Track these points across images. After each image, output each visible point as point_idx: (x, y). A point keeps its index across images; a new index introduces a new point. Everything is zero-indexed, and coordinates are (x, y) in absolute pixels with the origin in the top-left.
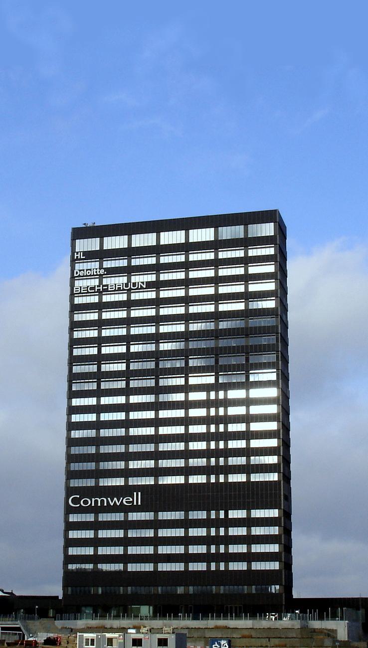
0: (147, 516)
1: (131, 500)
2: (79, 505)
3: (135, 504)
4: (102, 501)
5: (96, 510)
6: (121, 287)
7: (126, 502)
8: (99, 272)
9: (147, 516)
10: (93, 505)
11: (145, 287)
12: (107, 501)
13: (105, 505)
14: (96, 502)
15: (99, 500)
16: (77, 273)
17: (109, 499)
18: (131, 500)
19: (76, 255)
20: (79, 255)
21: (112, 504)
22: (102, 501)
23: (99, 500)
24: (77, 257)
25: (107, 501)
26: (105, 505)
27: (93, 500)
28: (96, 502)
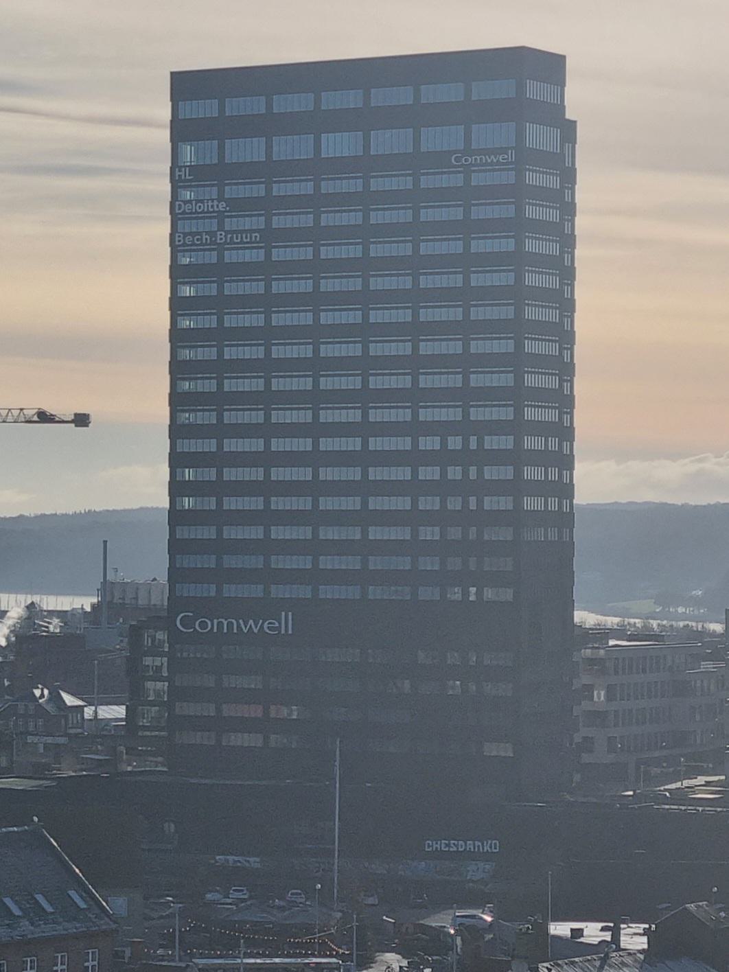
1: (277, 625)
2: (192, 630)
3: (283, 632)
4: (230, 625)
7: (268, 627)
8: (218, 206)
10: (215, 630)
12: (238, 622)
13: (235, 631)
14: (220, 624)
15: (225, 623)
17: (241, 621)
18: (277, 625)
20: (183, 173)
22: (230, 625)
23: (225, 623)
25: (238, 622)
27: (215, 621)
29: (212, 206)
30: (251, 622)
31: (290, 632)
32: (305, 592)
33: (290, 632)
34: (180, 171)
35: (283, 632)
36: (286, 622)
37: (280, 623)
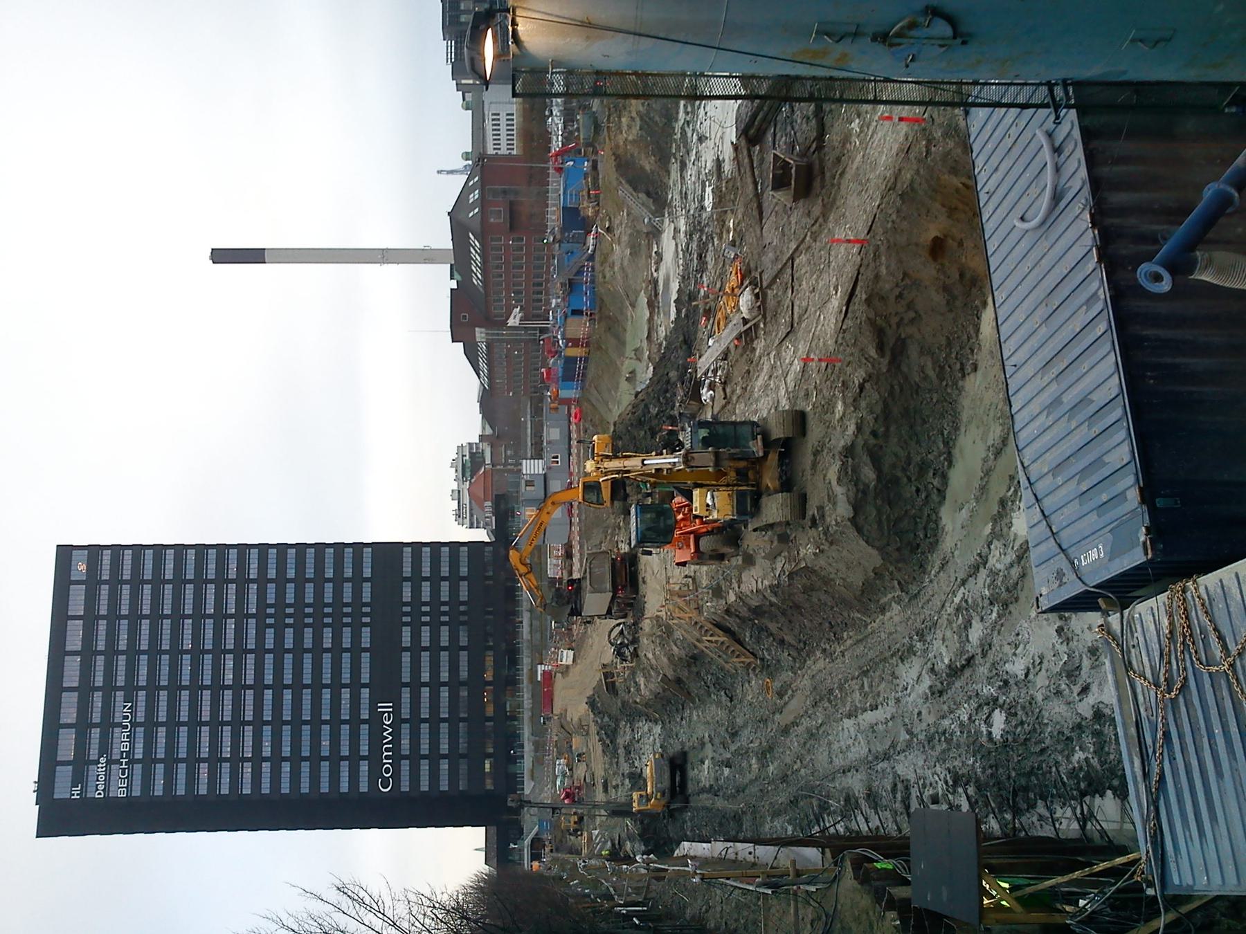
0: (406, 694)
1: (386, 714)
3: (391, 710)
4: (387, 750)
5: (397, 758)
6: (126, 734)
7: (389, 720)
9: (406, 694)
10: (391, 761)
11: (130, 704)
12: (386, 743)
13: (391, 746)
14: (387, 758)
15: (386, 754)
16: (100, 794)
18: (386, 714)
19: (75, 797)
20: (76, 793)
21: (391, 738)
22: (387, 750)
23: (386, 754)
24: (78, 795)
25: (386, 743)
26: (391, 746)
27: (385, 761)
28: (387, 758)
29: (102, 768)
30: (385, 734)
31: (391, 704)
32: (365, 693)
33: (391, 704)
34: (73, 795)
35: (391, 710)
36: (385, 707)
37: (385, 712)
